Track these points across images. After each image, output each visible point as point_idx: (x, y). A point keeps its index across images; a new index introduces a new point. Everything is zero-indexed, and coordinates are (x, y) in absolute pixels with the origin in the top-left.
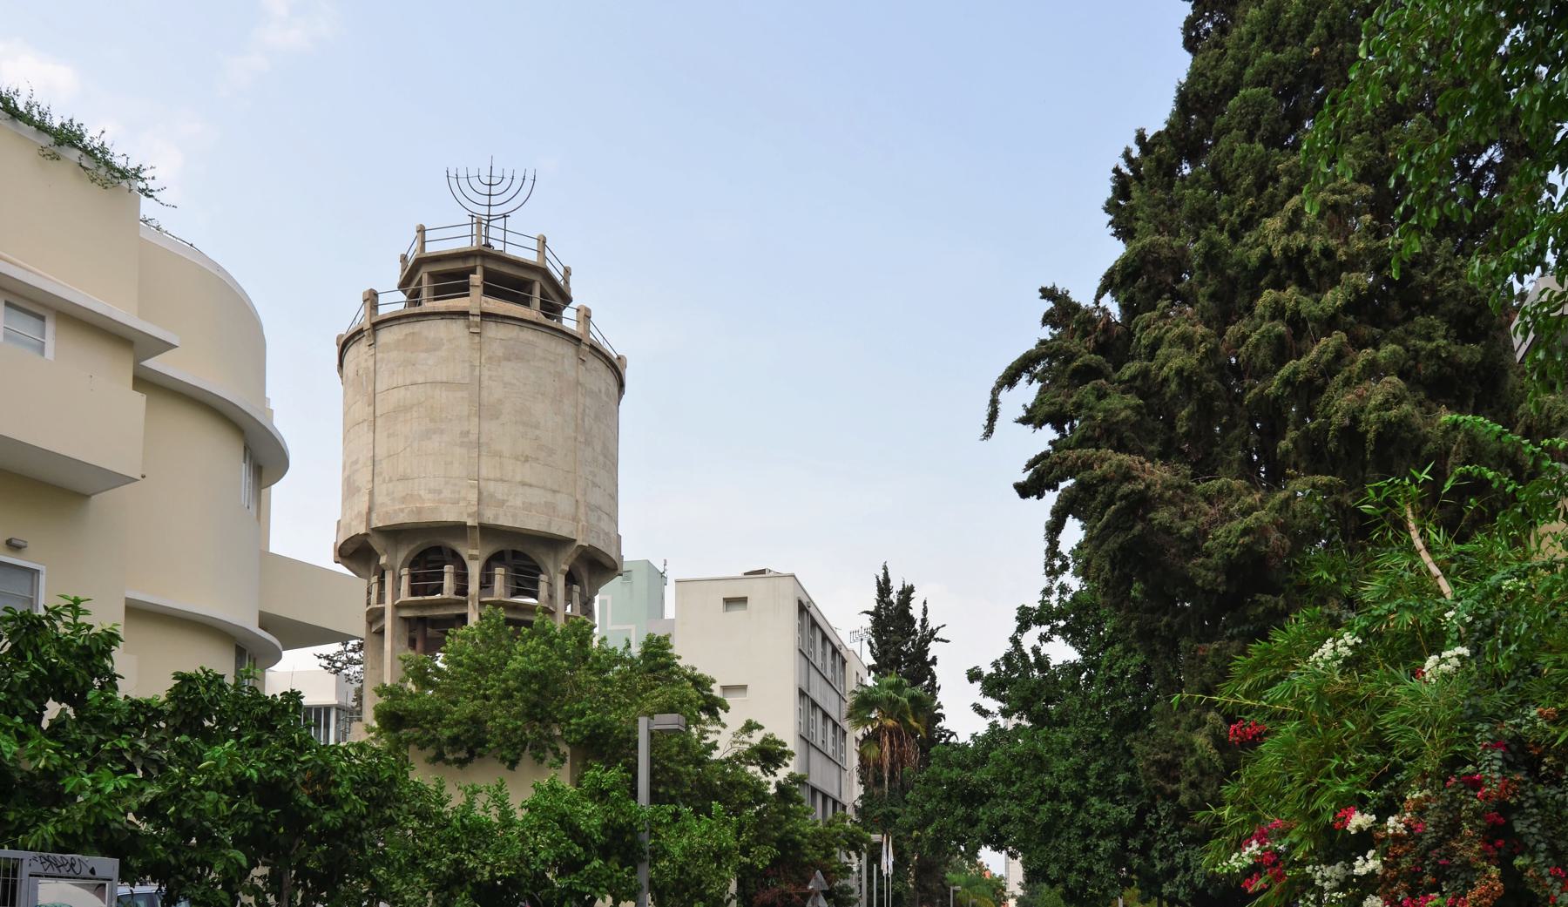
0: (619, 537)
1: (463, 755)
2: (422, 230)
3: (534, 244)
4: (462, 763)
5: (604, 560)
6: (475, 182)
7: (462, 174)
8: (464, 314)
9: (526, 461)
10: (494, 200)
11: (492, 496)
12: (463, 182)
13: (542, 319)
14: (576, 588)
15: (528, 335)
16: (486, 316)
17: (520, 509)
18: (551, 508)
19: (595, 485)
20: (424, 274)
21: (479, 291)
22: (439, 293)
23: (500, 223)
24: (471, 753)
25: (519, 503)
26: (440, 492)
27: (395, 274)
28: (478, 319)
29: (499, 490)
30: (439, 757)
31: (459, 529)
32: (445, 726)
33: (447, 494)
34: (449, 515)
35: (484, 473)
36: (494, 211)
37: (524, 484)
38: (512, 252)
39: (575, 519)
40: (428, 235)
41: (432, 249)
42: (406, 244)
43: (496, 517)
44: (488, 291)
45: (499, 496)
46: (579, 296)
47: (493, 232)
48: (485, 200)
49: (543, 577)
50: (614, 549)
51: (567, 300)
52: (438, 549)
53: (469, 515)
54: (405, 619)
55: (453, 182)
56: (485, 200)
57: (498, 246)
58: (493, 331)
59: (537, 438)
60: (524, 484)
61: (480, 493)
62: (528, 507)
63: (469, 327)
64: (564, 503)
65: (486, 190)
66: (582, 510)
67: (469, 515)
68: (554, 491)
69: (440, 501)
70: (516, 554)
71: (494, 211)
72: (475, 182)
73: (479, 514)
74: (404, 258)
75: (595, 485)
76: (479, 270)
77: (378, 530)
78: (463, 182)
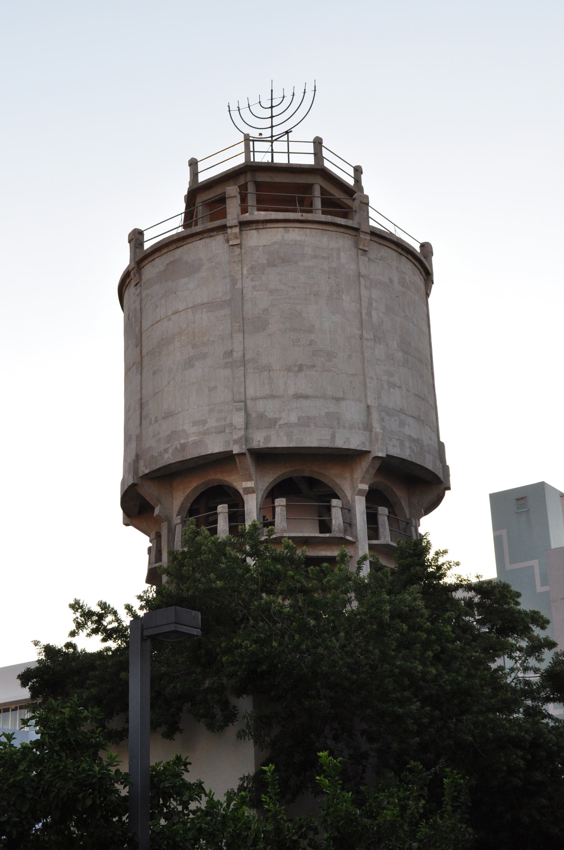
9: (301, 368)
11: (261, 416)
17: (296, 422)
18: (334, 421)
19: (392, 385)
25: (293, 419)
26: (204, 422)
29: (270, 408)
31: (225, 460)
33: (212, 423)
34: (215, 446)
35: (251, 392)
37: (298, 397)
43: (268, 439)
45: (270, 415)
53: (236, 442)
59: (311, 343)
60: (298, 397)
61: (247, 415)
62: (305, 422)
64: (352, 412)
66: (375, 416)
67: (236, 442)
68: (338, 400)
69: (206, 433)
73: (247, 439)
75: (392, 385)
77: (146, 477)
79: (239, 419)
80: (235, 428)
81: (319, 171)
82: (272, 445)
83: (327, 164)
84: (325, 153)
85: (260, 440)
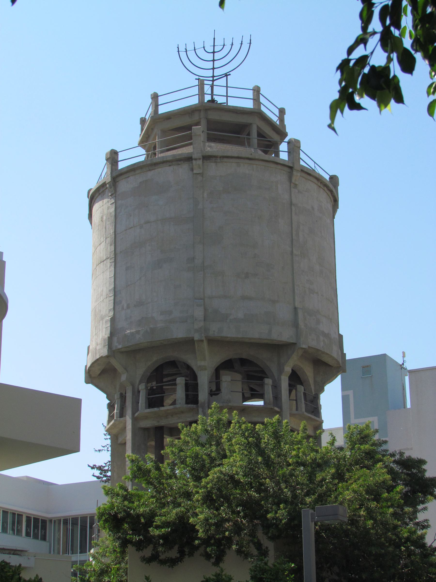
0: (341, 337)
1: (174, 553)
2: (155, 97)
3: (250, 94)
4: (172, 562)
5: (325, 359)
6: (201, 53)
7: (190, 48)
8: (189, 159)
10: (217, 64)
12: (192, 54)
13: (260, 154)
14: (301, 389)
15: (244, 169)
16: (207, 158)
20: (157, 131)
21: (203, 137)
22: (169, 145)
23: (223, 81)
24: (182, 554)
27: (136, 134)
28: (200, 162)
30: (153, 559)
31: (188, 343)
32: (157, 527)
34: (179, 332)
36: (217, 72)
37: (245, 298)
38: (232, 103)
39: (296, 325)
40: (161, 100)
41: (162, 110)
42: (145, 110)
44: (211, 139)
46: (292, 132)
47: (216, 90)
48: (210, 65)
49: (268, 382)
50: (335, 348)
51: (282, 134)
52: (173, 364)
54: (146, 430)
55: (183, 55)
56: (210, 65)
57: (220, 100)
58: (213, 170)
61: (206, 310)
63: (192, 170)
65: (210, 57)
70: (243, 362)
71: (217, 72)
72: (201, 53)
74: (143, 121)
76: (204, 122)
78: (192, 54)
79: (199, 313)
80: (196, 320)
81: (257, 113)
82: (224, 334)
83: (263, 109)
84: (262, 100)
85: (215, 330)
